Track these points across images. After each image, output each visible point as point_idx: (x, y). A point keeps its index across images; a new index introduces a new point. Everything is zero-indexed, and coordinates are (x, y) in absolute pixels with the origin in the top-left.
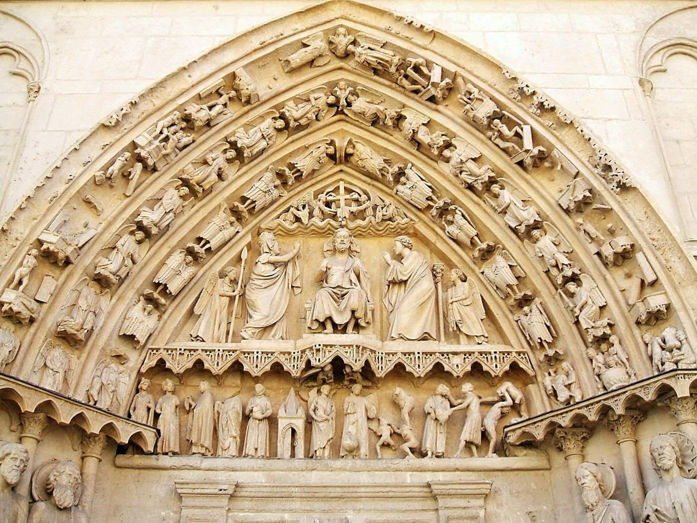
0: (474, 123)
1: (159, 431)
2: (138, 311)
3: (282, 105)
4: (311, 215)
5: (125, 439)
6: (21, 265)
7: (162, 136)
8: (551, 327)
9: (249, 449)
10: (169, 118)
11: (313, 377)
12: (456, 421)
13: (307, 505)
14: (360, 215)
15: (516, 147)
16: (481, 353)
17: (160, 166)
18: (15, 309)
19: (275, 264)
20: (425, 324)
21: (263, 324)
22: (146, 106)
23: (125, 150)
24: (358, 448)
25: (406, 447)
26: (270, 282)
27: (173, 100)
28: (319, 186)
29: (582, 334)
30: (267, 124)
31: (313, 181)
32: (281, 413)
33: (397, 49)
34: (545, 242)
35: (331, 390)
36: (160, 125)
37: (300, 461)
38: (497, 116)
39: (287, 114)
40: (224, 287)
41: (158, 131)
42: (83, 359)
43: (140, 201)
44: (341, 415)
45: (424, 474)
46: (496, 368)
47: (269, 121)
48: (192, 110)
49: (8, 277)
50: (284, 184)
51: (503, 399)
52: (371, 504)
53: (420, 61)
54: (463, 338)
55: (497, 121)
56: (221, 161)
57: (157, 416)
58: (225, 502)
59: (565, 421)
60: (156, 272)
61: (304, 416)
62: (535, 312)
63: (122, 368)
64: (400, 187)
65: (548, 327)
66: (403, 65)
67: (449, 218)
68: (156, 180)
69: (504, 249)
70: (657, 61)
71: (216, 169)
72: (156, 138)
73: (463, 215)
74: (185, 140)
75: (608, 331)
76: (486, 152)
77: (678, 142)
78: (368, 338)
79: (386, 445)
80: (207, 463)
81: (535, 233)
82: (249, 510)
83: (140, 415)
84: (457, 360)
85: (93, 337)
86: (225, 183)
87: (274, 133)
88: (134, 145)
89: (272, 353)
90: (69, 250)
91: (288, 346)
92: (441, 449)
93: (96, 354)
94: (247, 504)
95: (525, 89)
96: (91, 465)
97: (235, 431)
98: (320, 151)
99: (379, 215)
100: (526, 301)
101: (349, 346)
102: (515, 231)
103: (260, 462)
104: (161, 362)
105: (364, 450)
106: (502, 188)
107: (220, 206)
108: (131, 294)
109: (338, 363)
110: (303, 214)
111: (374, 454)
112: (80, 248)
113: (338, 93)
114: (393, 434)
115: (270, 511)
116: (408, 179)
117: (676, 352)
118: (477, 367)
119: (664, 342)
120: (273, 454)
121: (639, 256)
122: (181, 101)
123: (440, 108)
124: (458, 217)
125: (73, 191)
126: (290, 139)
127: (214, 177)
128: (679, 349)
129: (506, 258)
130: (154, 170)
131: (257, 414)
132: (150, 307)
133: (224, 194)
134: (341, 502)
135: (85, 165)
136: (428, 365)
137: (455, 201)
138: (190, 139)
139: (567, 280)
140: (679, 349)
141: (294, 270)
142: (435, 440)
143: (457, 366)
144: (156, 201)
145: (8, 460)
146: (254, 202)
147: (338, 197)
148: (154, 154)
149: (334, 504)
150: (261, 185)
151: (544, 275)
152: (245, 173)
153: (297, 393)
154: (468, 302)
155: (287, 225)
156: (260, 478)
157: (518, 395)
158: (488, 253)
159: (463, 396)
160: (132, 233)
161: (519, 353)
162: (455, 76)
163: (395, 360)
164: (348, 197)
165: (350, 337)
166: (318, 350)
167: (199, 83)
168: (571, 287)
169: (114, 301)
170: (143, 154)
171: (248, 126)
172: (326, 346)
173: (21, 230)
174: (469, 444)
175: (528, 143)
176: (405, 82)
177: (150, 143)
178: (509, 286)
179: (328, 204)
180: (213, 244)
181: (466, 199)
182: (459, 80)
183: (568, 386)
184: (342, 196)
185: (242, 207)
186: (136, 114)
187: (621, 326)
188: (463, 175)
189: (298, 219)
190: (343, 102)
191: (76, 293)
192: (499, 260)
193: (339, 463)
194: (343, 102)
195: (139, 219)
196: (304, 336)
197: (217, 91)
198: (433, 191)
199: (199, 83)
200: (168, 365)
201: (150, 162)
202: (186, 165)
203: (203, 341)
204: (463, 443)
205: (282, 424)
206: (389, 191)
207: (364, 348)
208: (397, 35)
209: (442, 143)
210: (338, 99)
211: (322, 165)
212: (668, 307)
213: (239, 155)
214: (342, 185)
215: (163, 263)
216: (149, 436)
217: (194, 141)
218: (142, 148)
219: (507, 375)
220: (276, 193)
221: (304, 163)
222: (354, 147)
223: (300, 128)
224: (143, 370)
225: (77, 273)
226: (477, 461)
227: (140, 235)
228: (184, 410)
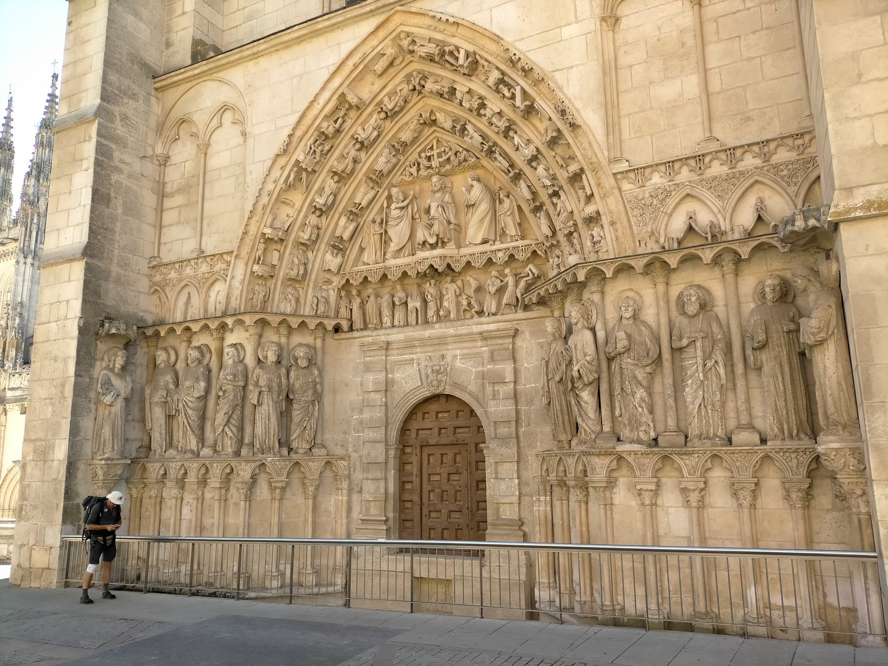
2: (329, 257)
3: (381, 102)
6: (257, 250)
7: (312, 151)
9: (396, 323)
12: (501, 290)
13: (423, 349)
17: (316, 169)
19: (402, 208)
21: (396, 248)
22: (299, 133)
23: (293, 166)
26: (399, 220)
27: (312, 124)
31: (418, 143)
35: (437, 281)
42: (305, 289)
45: (483, 326)
49: (253, 257)
50: (397, 151)
56: (353, 153)
58: (384, 352)
68: (318, 177)
71: (351, 158)
72: (309, 152)
73: (501, 155)
74: (327, 148)
78: (449, 250)
80: (375, 333)
82: (398, 355)
84: (500, 254)
86: (361, 165)
87: (382, 122)
88: (297, 162)
92: (493, 310)
93: (311, 284)
94: (396, 352)
108: (323, 246)
112: (286, 231)
115: (406, 354)
124: (497, 155)
125: (273, 200)
126: (394, 122)
130: (315, 171)
132: (335, 251)
134: (440, 346)
135: (275, 182)
136: (484, 259)
137: (495, 144)
138: (329, 146)
142: (491, 305)
144: (322, 189)
148: (310, 164)
149: (437, 348)
150: (382, 160)
152: (373, 152)
154: (508, 213)
160: (314, 213)
163: (465, 260)
165: (438, 252)
167: (323, 108)
169: (314, 253)
170: (304, 167)
173: (253, 229)
180: (364, 204)
186: (295, 140)
197: (337, 108)
198: (483, 139)
199: (323, 108)
200: (351, 282)
201: (309, 170)
202: (333, 162)
203: (368, 264)
205: (411, 305)
207: (445, 257)
209: (476, 107)
211: (420, 133)
215: (337, 224)
217: (332, 147)
220: (394, 160)
223: (397, 113)
224: (340, 287)
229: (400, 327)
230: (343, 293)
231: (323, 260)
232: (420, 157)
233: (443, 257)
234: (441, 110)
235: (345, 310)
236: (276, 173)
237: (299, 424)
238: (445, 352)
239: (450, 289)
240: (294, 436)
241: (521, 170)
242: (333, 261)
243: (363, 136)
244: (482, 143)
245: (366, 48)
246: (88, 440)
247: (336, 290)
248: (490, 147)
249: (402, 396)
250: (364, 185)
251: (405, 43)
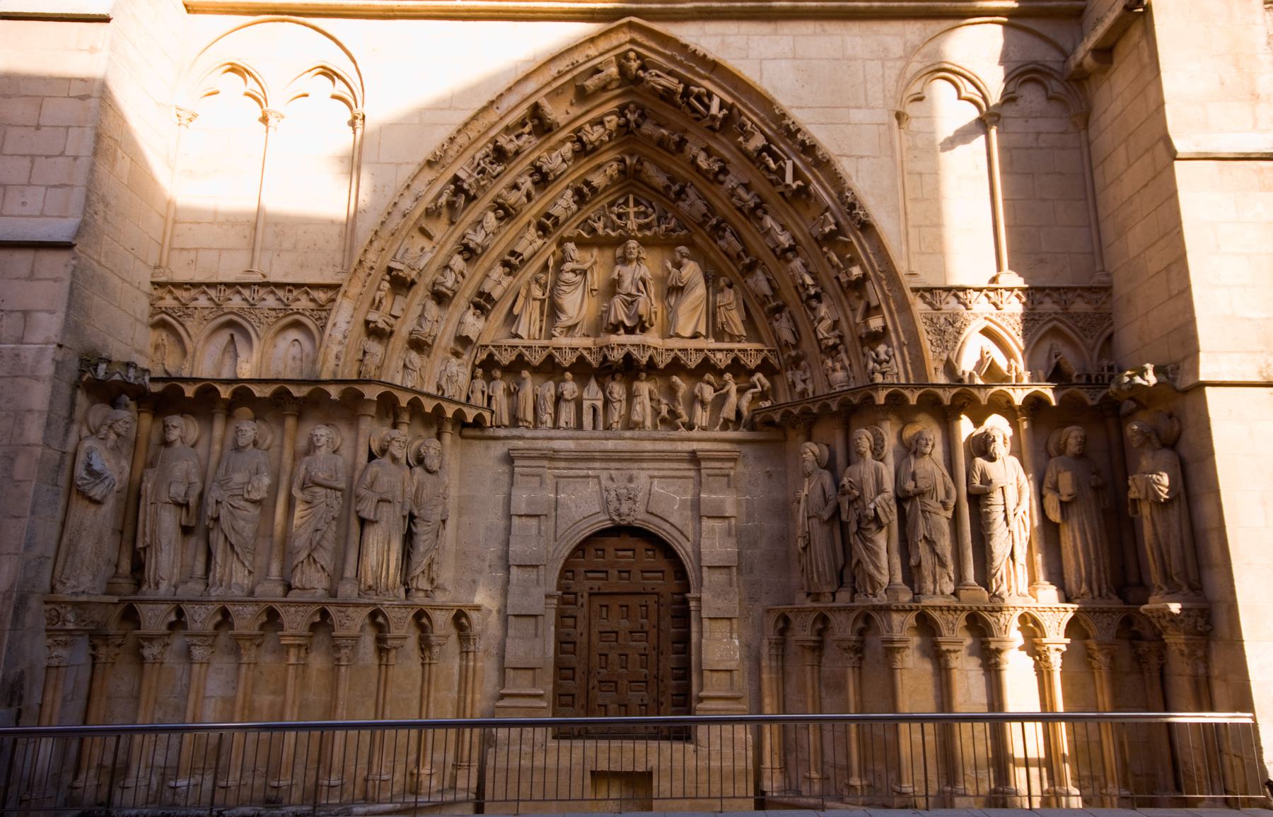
0: (744, 152)
1: (493, 412)
2: (470, 318)
3: (580, 129)
4: (605, 227)
5: (470, 420)
8: (796, 333)
9: (562, 424)
10: (483, 152)
11: (610, 367)
13: (604, 465)
14: (648, 226)
15: (780, 180)
16: (739, 350)
17: (480, 195)
18: (381, 325)
20: (696, 326)
21: (570, 323)
24: (643, 422)
25: (679, 422)
26: (573, 287)
28: (611, 198)
29: (819, 341)
30: (567, 148)
32: (585, 395)
33: (681, 79)
34: (797, 263)
36: (479, 156)
37: (600, 432)
38: (766, 149)
39: (585, 138)
40: (537, 292)
41: (475, 164)
43: (464, 225)
44: (631, 396)
46: (752, 363)
47: (569, 145)
48: (502, 141)
49: (371, 299)
51: (755, 387)
52: (651, 465)
53: (703, 90)
54: (727, 339)
55: (764, 154)
57: (490, 398)
59: (796, 411)
60: (482, 283)
61: (602, 398)
62: (784, 319)
63: (460, 361)
64: (681, 203)
65: (793, 333)
66: (686, 93)
67: (721, 233)
69: (764, 264)
70: (916, 88)
73: (732, 233)
74: (499, 169)
75: (838, 341)
76: (754, 180)
77: (920, 174)
79: (663, 421)
80: (529, 434)
81: (790, 255)
82: (564, 469)
83: (478, 399)
84: (719, 355)
85: (437, 340)
88: (456, 179)
89: (577, 349)
90: (414, 274)
91: (589, 342)
94: (562, 464)
95: (791, 127)
96: (447, 438)
97: (550, 409)
98: (612, 169)
99: (663, 227)
100: (779, 309)
101: (638, 345)
102: (773, 251)
103: (570, 433)
104: (491, 355)
105: (648, 423)
106: (766, 212)
107: (529, 223)
109: (628, 357)
110: (599, 226)
111: (655, 427)
113: (629, 116)
114: (670, 412)
116: (687, 196)
117: (884, 365)
118: (736, 360)
119: (877, 355)
120: (580, 426)
121: (869, 285)
122: (492, 133)
123: (718, 135)
124: (728, 234)
125: (411, 223)
127: (525, 199)
128: (888, 362)
129: (765, 273)
130: (475, 198)
131: (567, 395)
133: (531, 212)
138: (502, 168)
139: (810, 297)
140: (888, 362)
141: (592, 275)
142: (702, 417)
143: (722, 360)
145: (394, 442)
146: (557, 218)
147: (628, 210)
149: (625, 465)
151: (793, 290)
153: (597, 381)
155: (584, 234)
156: (571, 445)
157: (767, 384)
158: (750, 269)
159: (726, 383)
160: (460, 253)
161: (769, 351)
162: (731, 108)
164: (636, 209)
165: (636, 338)
166: (613, 349)
167: (506, 115)
168: (814, 303)
169: (450, 309)
170: (466, 186)
171: (553, 149)
172: (619, 345)
174: (727, 421)
175: (789, 178)
176: (688, 110)
177: (470, 176)
178: (765, 296)
179: (620, 216)
180: (526, 255)
181: (738, 220)
182: (735, 111)
183: (804, 381)
184: (632, 210)
185: (549, 223)
187: (848, 338)
188: (734, 200)
189: (593, 231)
190: (633, 125)
191: (421, 307)
192: (759, 274)
193: (628, 434)
194: (633, 125)
195: (465, 241)
196: (602, 335)
197: (524, 119)
198: (708, 209)
199: (506, 115)
201: (472, 192)
202: (500, 188)
204: (722, 420)
205: (586, 404)
206: (671, 204)
207: (649, 347)
208: (680, 64)
210: (628, 121)
212: (885, 328)
213: (543, 179)
214: (631, 198)
216: (487, 415)
218: (463, 181)
219: (759, 369)
221: (598, 180)
222: (642, 164)
224: (477, 362)
225: (421, 292)
226: (731, 434)
227: (467, 255)
228: (511, 394)
230: (479, 371)
231: (461, 323)
233: (645, 347)
234: (653, 161)
235: (479, 395)
236: (419, 186)
238: (635, 472)
239: (644, 388)
240: (419, 570)
241: (758, 258)
242: (473, 325)
243: (551, 166)
244: (704, 215)
245: (579, 57)
246: (49, 558)
247: (470, 367)
248: (719, 223)
249: (570, 524)
250: (532, 230)
251: (634, 65)
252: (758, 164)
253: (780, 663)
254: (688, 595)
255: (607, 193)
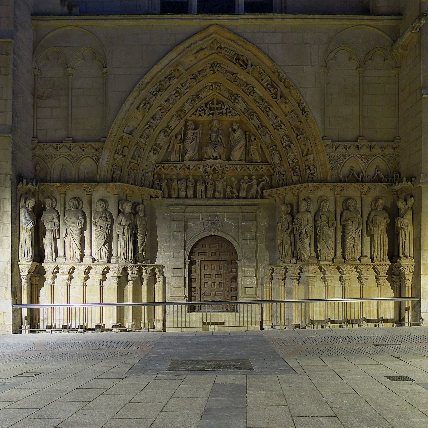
8: (281, 160)
9: (189, 196)
25: (234, 195)
51: (264, 181)
92: (244, 196)
164: (217, 106)
180: (173, 127)
229: (191, 198)
232: (206, 107)
237: (141, 247)
252: (267, 89)
253: (271, 285)
254: (237, 261)
255: (205, 99)
